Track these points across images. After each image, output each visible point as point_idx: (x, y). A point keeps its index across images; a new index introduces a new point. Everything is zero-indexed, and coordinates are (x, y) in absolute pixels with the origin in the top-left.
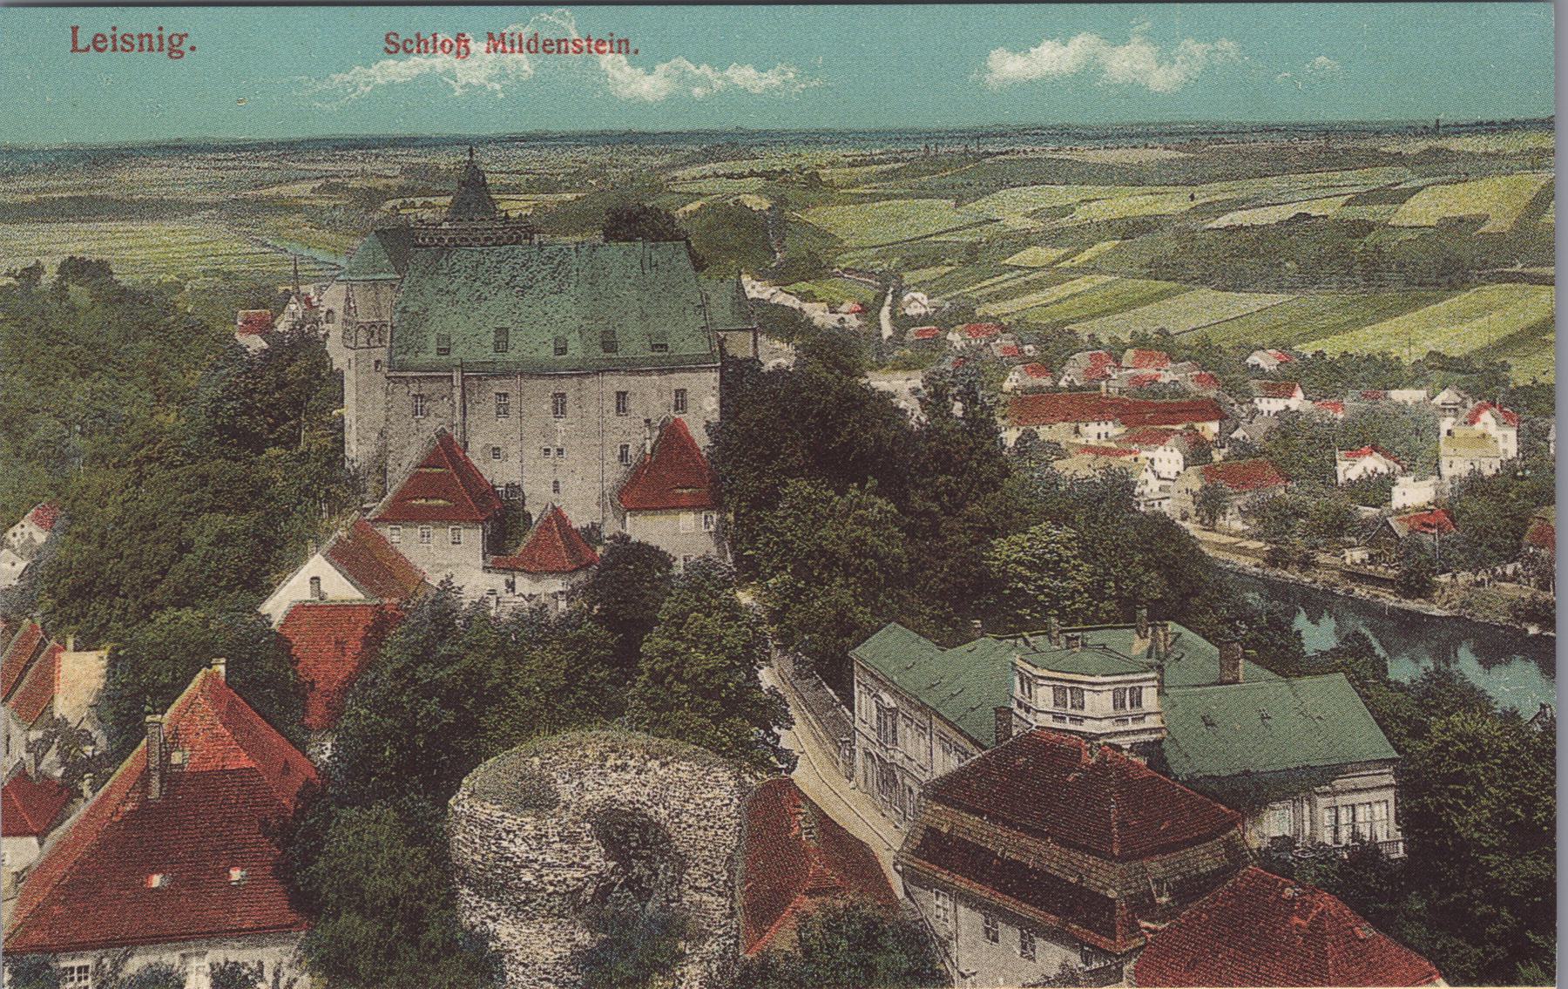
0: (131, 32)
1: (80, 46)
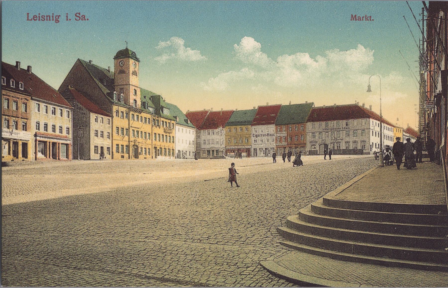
0: (44, 15)
1: (30, 19)
